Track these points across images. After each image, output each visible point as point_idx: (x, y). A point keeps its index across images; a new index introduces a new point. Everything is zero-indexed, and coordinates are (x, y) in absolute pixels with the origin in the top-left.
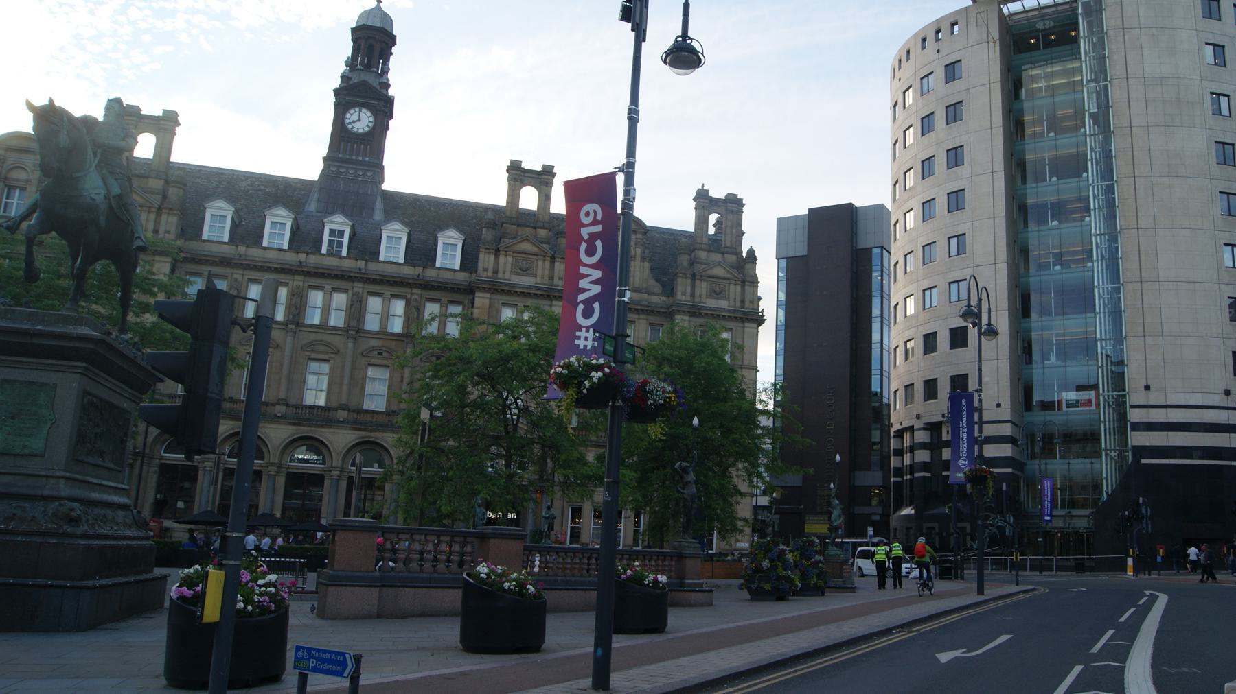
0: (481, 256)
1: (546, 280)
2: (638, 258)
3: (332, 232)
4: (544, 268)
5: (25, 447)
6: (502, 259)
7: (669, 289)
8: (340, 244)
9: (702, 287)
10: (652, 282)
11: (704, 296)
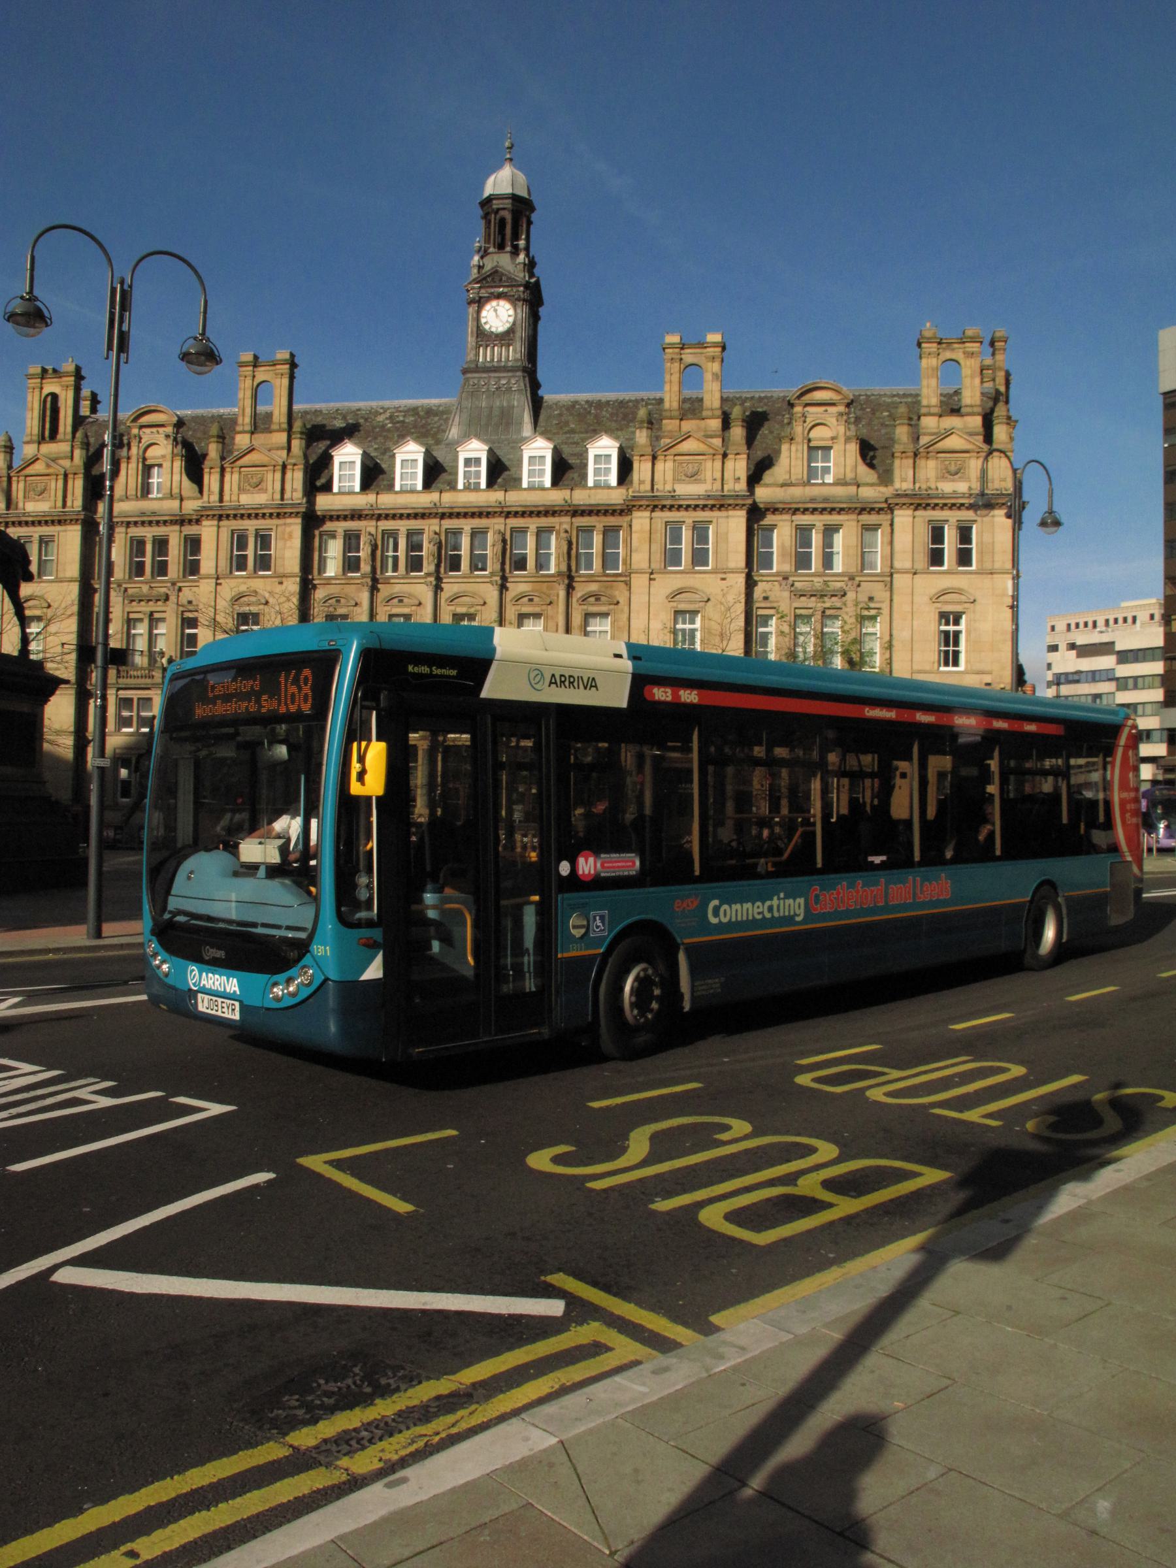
0: (636, 465)
1: (718, 485)
2: (842, 440)
3: (468, 462)
6: (659, 466)
8: (478, 474)
9: (929, 469)
10: (863, 469)
11: (933, 480)
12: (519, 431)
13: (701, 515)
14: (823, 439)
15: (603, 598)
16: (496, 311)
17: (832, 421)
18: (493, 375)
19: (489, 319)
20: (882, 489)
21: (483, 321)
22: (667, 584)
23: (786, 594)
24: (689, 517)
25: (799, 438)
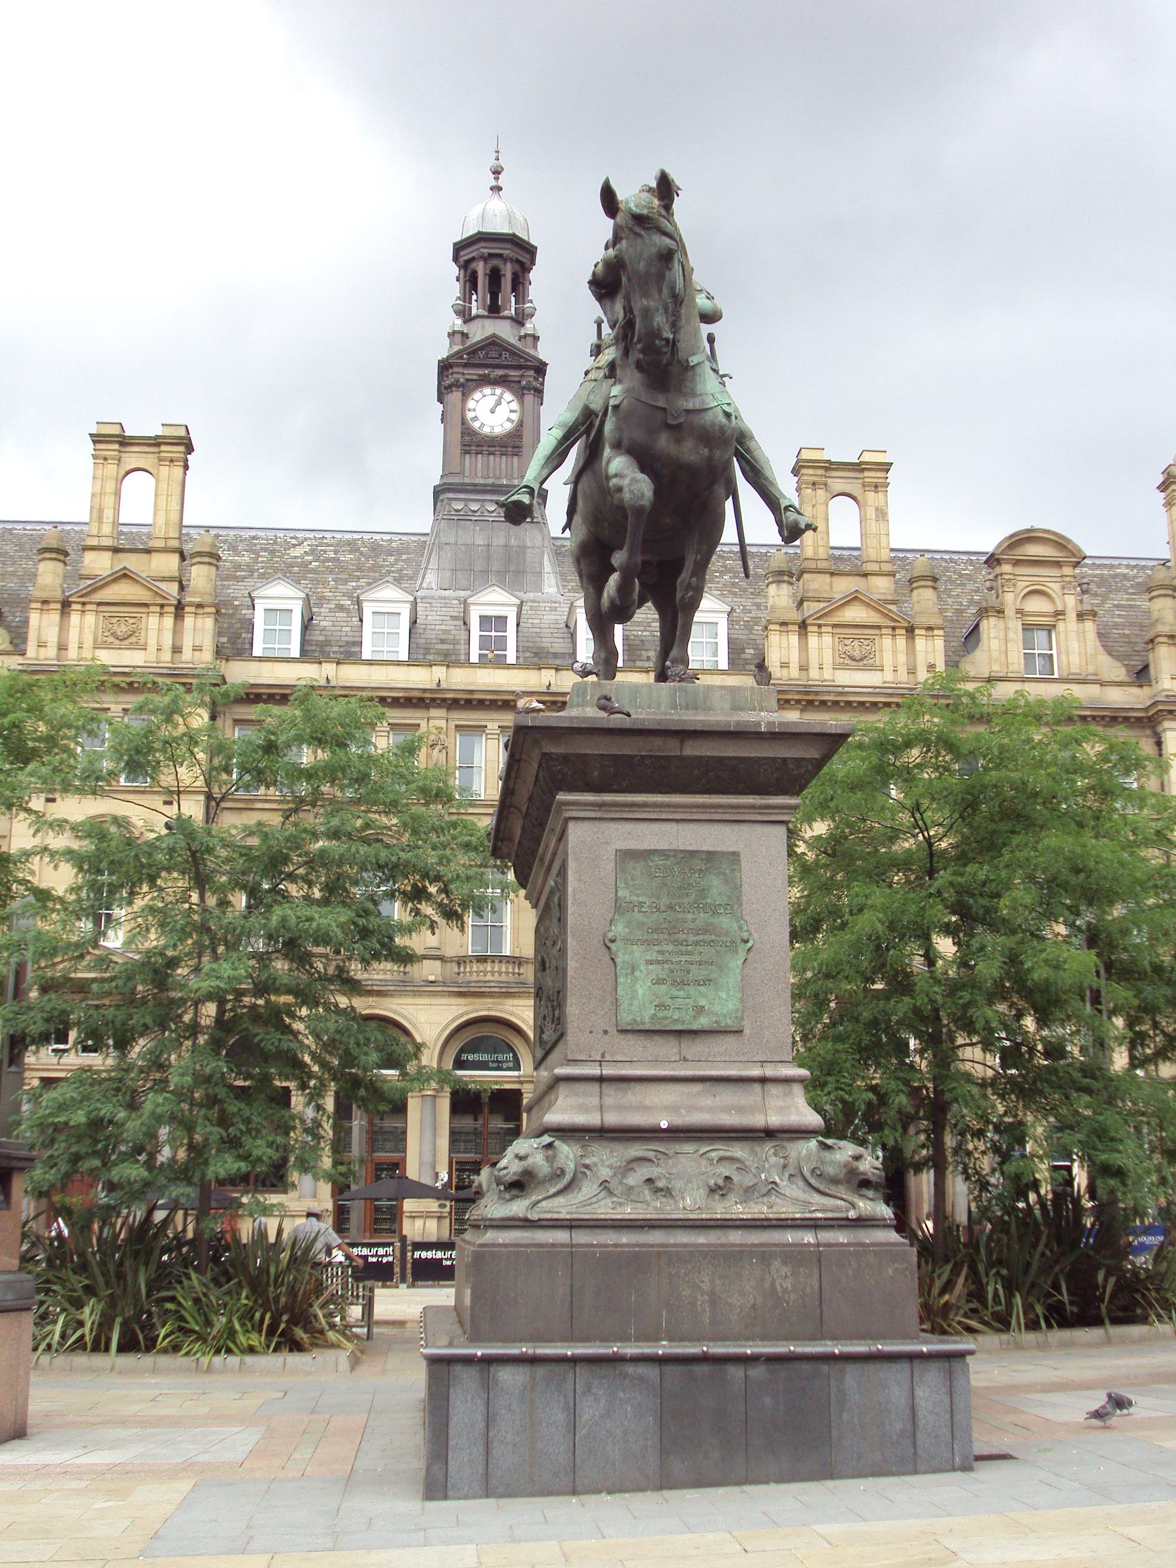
2: (1072, 616)
3: (485, 620)
4: (895, 652)
5: (700, 1010)
6: (813, 640)
7: (1142, 675)
8: (502, 643)
12: (539, 588)
16: (498, 403)
17: (1054, 588)
18: (488, 497)
19: (478, 413)
20: (1135, 690)
21: (470, 415)
25: (1010, 612)
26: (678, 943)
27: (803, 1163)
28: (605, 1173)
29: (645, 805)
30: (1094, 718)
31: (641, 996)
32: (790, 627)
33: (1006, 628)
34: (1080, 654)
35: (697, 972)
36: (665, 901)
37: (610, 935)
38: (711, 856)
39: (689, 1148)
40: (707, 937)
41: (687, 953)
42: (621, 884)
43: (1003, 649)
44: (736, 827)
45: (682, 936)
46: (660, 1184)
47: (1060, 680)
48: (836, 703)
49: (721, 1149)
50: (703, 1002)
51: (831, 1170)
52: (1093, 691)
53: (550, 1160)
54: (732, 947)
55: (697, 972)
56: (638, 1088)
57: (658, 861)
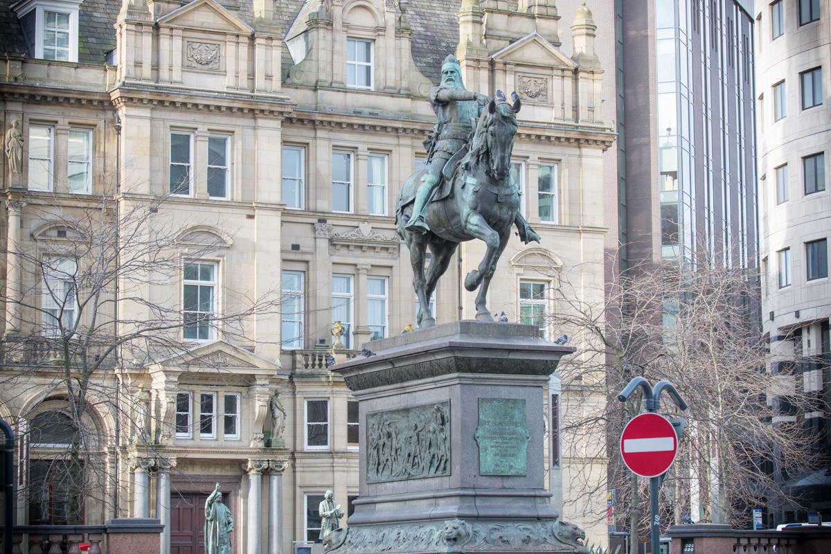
1: (244, 82)
2: (391, 32)
5: (511, 467)
6: (165, 43)
13: (222, 122)
14: (364, 29)
15: (69, 234)
22: (176, 219)
23: (323, 244)
24: (203, 125)
25: (337, 25)
26: (503, 438)
27: (554, 531)
28: (483, 534)
29: (491, 379)
30: (405, 130)
31: (489, 461)
32: (145, 29)
33: (333, 41)
34: (396, 69)
35: (511, 451)
36: (498, 420)
37: (477, 435)
38: (515, 401)
39: (510, 524)
40: (514, 436)
41: (507, 443)
42: (481, 413)
43: (329, 59)
44: (524, 388)
45: (504, 436)
46: (505, 539)
47: (378, 93)
48: (184, 104)
49: (523, 525)
50: (512, 464)
51: (566, 534)
52: (406, 103)
53: (465, 528)
54: (523, 440)
55: (511, 451)
56: (494, 499)
57: (496, 403)
